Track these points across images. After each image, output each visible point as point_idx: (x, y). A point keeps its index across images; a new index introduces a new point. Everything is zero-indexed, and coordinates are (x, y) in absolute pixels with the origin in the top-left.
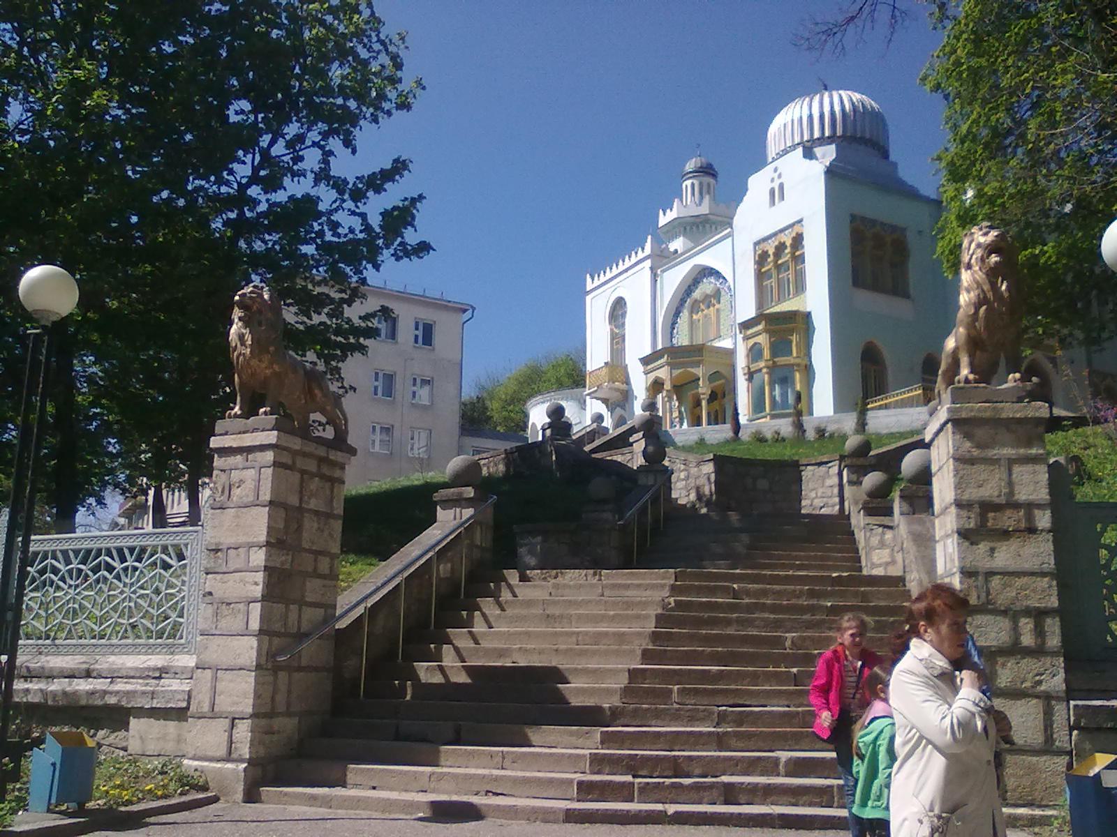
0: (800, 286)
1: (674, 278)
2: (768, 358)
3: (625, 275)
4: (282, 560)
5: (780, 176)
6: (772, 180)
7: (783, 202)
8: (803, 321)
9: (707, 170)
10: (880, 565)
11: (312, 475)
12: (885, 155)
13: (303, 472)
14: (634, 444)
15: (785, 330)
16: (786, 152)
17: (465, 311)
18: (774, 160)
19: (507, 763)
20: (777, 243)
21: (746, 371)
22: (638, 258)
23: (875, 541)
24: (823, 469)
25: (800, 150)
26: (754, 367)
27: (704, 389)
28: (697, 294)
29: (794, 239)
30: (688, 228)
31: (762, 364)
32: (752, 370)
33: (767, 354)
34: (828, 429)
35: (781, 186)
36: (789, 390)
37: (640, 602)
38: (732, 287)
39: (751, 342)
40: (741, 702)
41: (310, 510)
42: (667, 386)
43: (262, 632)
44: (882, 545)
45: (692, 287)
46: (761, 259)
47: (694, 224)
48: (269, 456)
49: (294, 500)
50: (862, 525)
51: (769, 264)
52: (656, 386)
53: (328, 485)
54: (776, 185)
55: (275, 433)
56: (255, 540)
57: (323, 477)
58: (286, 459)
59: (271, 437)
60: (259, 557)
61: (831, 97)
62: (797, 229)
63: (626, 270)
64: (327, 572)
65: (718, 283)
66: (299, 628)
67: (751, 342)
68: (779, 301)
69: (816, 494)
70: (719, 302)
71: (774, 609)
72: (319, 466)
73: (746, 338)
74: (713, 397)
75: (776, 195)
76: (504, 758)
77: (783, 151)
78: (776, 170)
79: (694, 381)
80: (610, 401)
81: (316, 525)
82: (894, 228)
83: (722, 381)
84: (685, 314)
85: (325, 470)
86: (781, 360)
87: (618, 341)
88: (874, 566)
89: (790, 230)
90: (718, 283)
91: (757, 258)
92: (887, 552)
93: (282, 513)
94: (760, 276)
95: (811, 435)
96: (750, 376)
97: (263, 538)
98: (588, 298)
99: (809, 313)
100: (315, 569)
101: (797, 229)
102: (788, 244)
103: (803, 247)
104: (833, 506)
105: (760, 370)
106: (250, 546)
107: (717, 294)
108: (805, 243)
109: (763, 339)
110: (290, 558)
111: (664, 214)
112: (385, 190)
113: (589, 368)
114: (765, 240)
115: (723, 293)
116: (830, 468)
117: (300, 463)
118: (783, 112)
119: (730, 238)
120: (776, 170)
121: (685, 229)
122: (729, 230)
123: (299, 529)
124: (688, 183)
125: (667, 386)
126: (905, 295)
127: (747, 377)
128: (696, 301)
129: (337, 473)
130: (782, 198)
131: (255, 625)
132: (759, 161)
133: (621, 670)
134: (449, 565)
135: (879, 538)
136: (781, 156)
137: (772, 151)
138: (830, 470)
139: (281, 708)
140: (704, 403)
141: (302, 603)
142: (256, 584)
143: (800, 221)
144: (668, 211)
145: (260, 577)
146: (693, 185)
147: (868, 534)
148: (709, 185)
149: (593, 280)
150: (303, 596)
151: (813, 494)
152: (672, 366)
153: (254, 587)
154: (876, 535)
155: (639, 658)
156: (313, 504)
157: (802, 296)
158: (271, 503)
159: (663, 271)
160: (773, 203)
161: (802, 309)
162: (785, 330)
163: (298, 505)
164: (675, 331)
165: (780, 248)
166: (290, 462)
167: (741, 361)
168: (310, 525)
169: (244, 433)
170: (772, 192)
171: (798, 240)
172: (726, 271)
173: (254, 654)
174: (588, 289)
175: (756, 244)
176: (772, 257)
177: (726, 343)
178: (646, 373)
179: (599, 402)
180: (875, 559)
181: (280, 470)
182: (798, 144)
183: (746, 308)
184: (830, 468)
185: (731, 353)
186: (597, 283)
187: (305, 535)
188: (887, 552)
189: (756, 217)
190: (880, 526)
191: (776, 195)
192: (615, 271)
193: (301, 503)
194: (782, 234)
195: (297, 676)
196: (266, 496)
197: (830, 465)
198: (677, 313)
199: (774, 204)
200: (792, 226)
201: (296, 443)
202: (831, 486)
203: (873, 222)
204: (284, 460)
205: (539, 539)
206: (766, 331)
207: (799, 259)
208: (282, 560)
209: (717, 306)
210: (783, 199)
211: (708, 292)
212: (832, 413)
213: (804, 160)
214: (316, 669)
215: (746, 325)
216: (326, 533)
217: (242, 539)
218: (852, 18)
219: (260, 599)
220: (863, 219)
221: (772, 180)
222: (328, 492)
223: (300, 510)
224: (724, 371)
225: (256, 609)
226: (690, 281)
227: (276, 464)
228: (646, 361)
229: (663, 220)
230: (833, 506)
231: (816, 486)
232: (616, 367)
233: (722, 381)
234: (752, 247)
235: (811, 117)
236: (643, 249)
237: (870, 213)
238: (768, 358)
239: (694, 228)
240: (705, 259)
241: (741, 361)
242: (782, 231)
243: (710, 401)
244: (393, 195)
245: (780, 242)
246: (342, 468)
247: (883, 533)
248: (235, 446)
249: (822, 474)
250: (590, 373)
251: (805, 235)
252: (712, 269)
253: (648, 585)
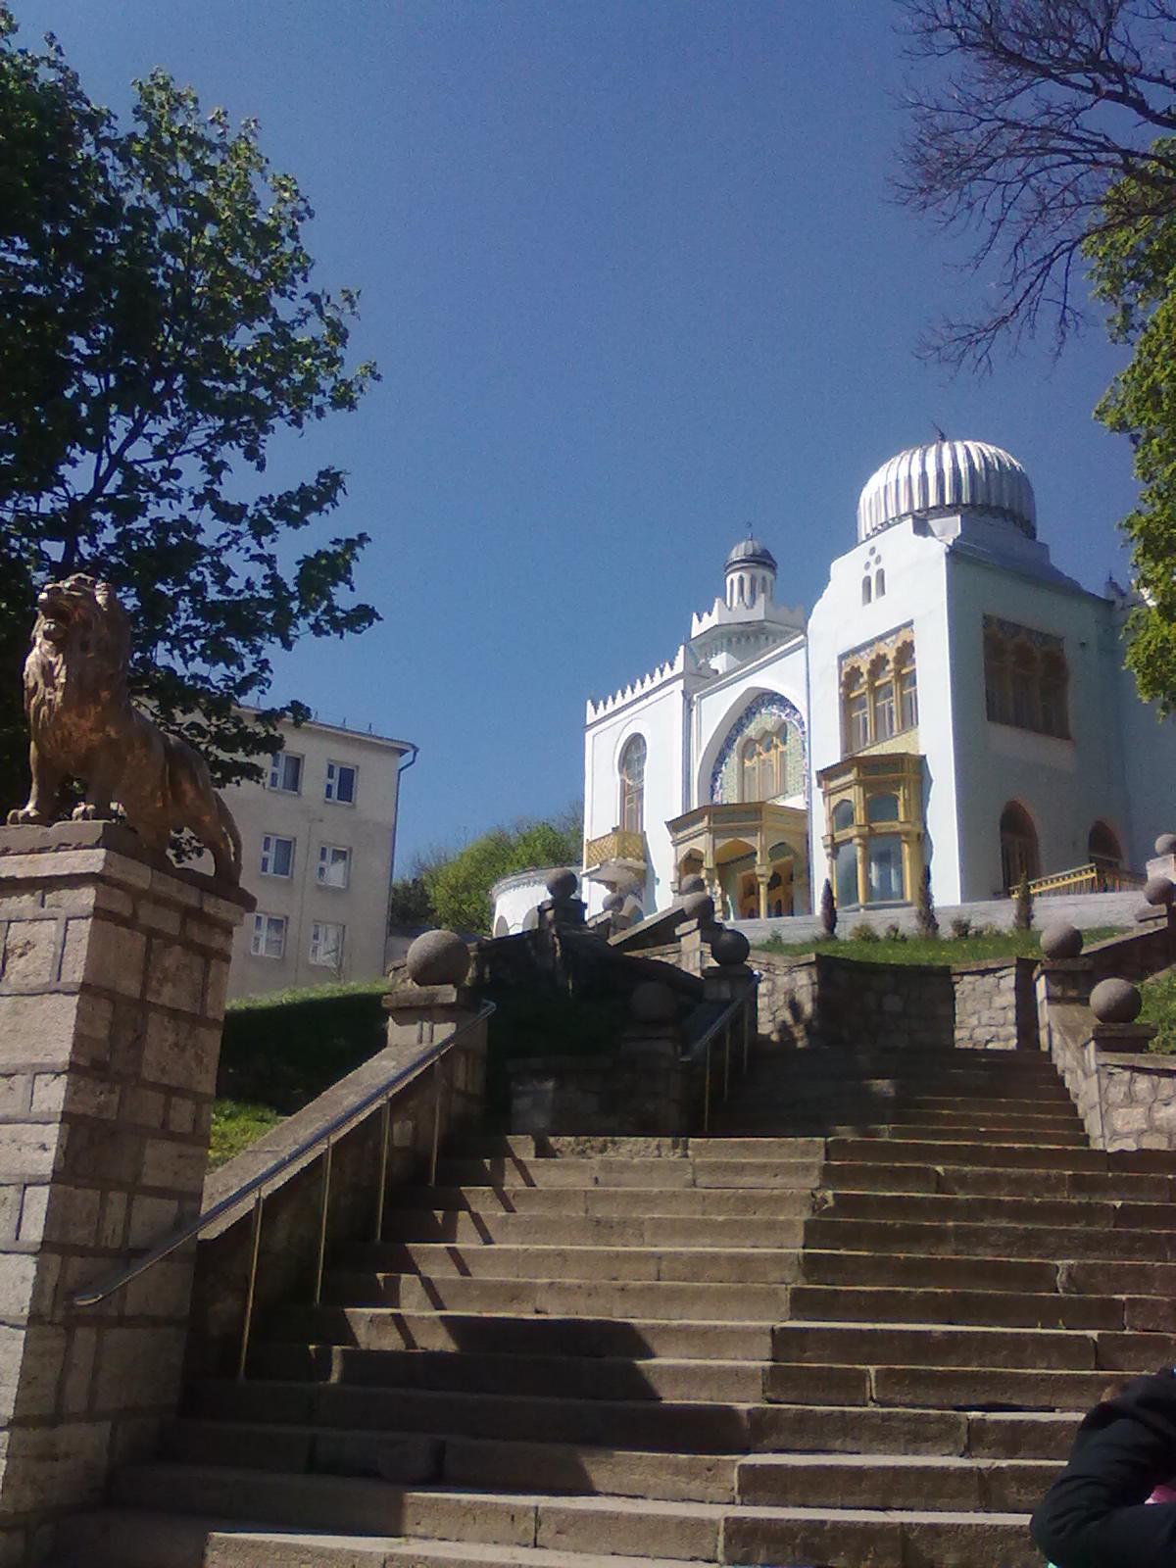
0: (909, 717)
1: (716, 708)
2: (863, 823)
3: (645, 702)
4: (100, 1100)
5: (878, 560)
6: (867, 566)
7: (883, 598)
8: (913, 771)
9: (761, 560)
10: (1127, 1135)
11: (170, 941)
12: (1031, 533)
13: (151, 933)
14: (683, 939)
15: (885, 782)
16: (887, 525)
17: (402, 752)
18: (869, 537)
19: (545, 1535)
20: (873, 657)
21: (829, 842)
22: (665, 678)
23: (1117, 1093)
24: (990, 980)
25: (909, 522)
26: (840, 836)
27: (762, 869)
28: (752, 730)
29: (900, 651)
30: (734, 640)
31: (852, 831)
32: (837, 840)
33: (859, 816)
34: (973, 924)
35: (881, 575)
36: (893, 871)
37: (770, 1198)
38: (805, 719)
39: (836, 799)
40: (1003, 1400)
41: (162, 1006)
42: (709, 863)
43: (46, 1246)
44: (1131, 1099)
45: (744, 721)
46: (850, 679)
47: (742, 633)
48: (87, 897)
49: (131, 986)
50: (1093, 1066)
51: (861, 688)
52: (690, 863)
53: (199, 961)
54: (872, 573)
55: (101, 852)
56: (48, 1060)
57: (189, 945)
58: (121, 905)
59: (93, 860)
60: (53, 1094)
61: (953, 449)
62: (904, 635)
63: (646, 695)
64: (187, 1127)
65: (784, 717)
66: (126, 1239)
67: (836, 799)
68: (877, 740)
69: (979, 1020)
70: (784, 742)
71: (1017, 1212)
72: (183, 923)
73: (828, 793)
74: (775, 882)
75: (873, 587)
76: (538, 1522)
77: (882, 525)
78: (872, 551)
79: (747, 856)
80: (619, 886)
81: (171, 1038)
82: (1046, 638)
83: (789, 858)
84: (733, 759)
85: (196, 933)
86: (882, 826)
87: (632, 797)
88: (1116, 1135)
89: (894, 637)
90: (784, 717)
91: (843, 679)
92: (1139, 1112)
93: (104, 1009)
94: (848, 704)
95: (946, 931)
96: (835, 848)
97: (63, 1055)
98: (589, 735)
99: (924, 757)
100: (164, 1124)
101: (904, 635)
102: (890, 657)
103: (914, 662)
104: (1007, 1039)
105: (850, 840)
106: (38, 1071)
107: (782, 731)
108: (916, 655)
109: (854, 795)
110: (115, 1098)
111: (700, 620)
112: (306, 523)
113: (587, 836)
114: (856, 651)
115: (789, 727)
116: (1001, 978)
117: (147, 915)
118: (882, 470)
119: (803, 650)
120: (872, 551)
121: (730, 640)
122: (802, 637)
123: (139, 1041)
124: (735, 576)
125: (709, 863)
126: (1064, 735)
127: (829, 850)
128: (751, 740)
129: (217, 941)
130: (882, 590)
131: (34, 1231)
132: (847, 540)
133: (760, 1331)
134: (410, 1124)
135: (1124, 1089)
136: (880, 532)
137: (865, 525)
138: (1002, 981)
139: (76, 1402)
140: (763, 889)
141: (135, 1189)
142: (44, 1147)
143: (910, 624)
144: (706, 615)
145: (52, 1134)
146: (741, 579)
147: (1105, 1082)
148: (764, 579)
149: (596, 708)
150: (138, 1176)
151: (974, 1021)
152: (716, 833)
153: (38, 1155)
154: (1121, 1082)
155: (785, 1307)
156: (167, 995)
157: (912, 733)
158: (85, 988)
159: (701, 697)
160: (867, 598)
161: (912, 752)
162: (885, 782)
163: (138, 996)
164: (718, 784)
165: (879, 663)
166: (127, 912)
167: (820, 827)
168: (160, 1037)
169: (41, 851)
170: (867, 583)
171: (906, 652)
172: (794, 694)
173: (27, 1292)
174: (589, 722)
175: (842, 657)
176: (866, 676)
177: (796, 802)
178: (676, 844)
179: (603, 887)
180: (1119, 1124)
181: (110, 926)
182: (905, 515)
183: (827, 749)
184: (1001, 978)
185: (802, 816)
186: (602, 712)
187: (149, 1054)
188: (1139, 1112)
189: (842, 619)
190: (1124, 1067)
191: (873, 587)
192: (629, 696)
193: (143, 992)
194: (882, 644)
195: (116, 1336)
196: (75, 973)
197: (1002, 973)
198: (721, 759)
199: (869, 600)
200: (896, 631)
201: (141, 876)
202: (1004, 1008)
203: (1017, 628)
204: (115, 907)
205: (550, 1085)
206: (858, 782)
207: (907, 679)
208: (100, 1100)
209: (782, 748)
210: (883, 592)
211: (769, 727)
212: (958, 901)
213: (915, 536)
214: (154, 1322)
215: (826, 775)
216: (190, 1053)
217: (21, 1058)
218: (1005, 320)
219: (49, 1179)
220: (1002, 623)
221: (867, 566)
222: (197, 975)
223: (142, 1005)
224: (791, 842)
225: (39, 1200)
226: (741, 712)
227: (99, 913)
228: (675, 826)
229: (698, 628)
230: (1007, 1039)
231: (978, 1007)
232: (629, 835)
233: (789, 858)
234: (835, 662)
235: (924, 475)
236: (672, 666)
237: (1012, 615)
238: (863, 823)
239: (743, 640)
240: (764, 680)
241: (820, 827)
242: (881, 638)
243: (771, 887)
244: (317, 535)
245: (878, 656)
246: (228, 932)
247: (1132, 1081)
248: (19, 876)
249: (987, 988)
250: (590, 843)
251: (915, 644)
252: (777, 694)
253: (779, 1166)
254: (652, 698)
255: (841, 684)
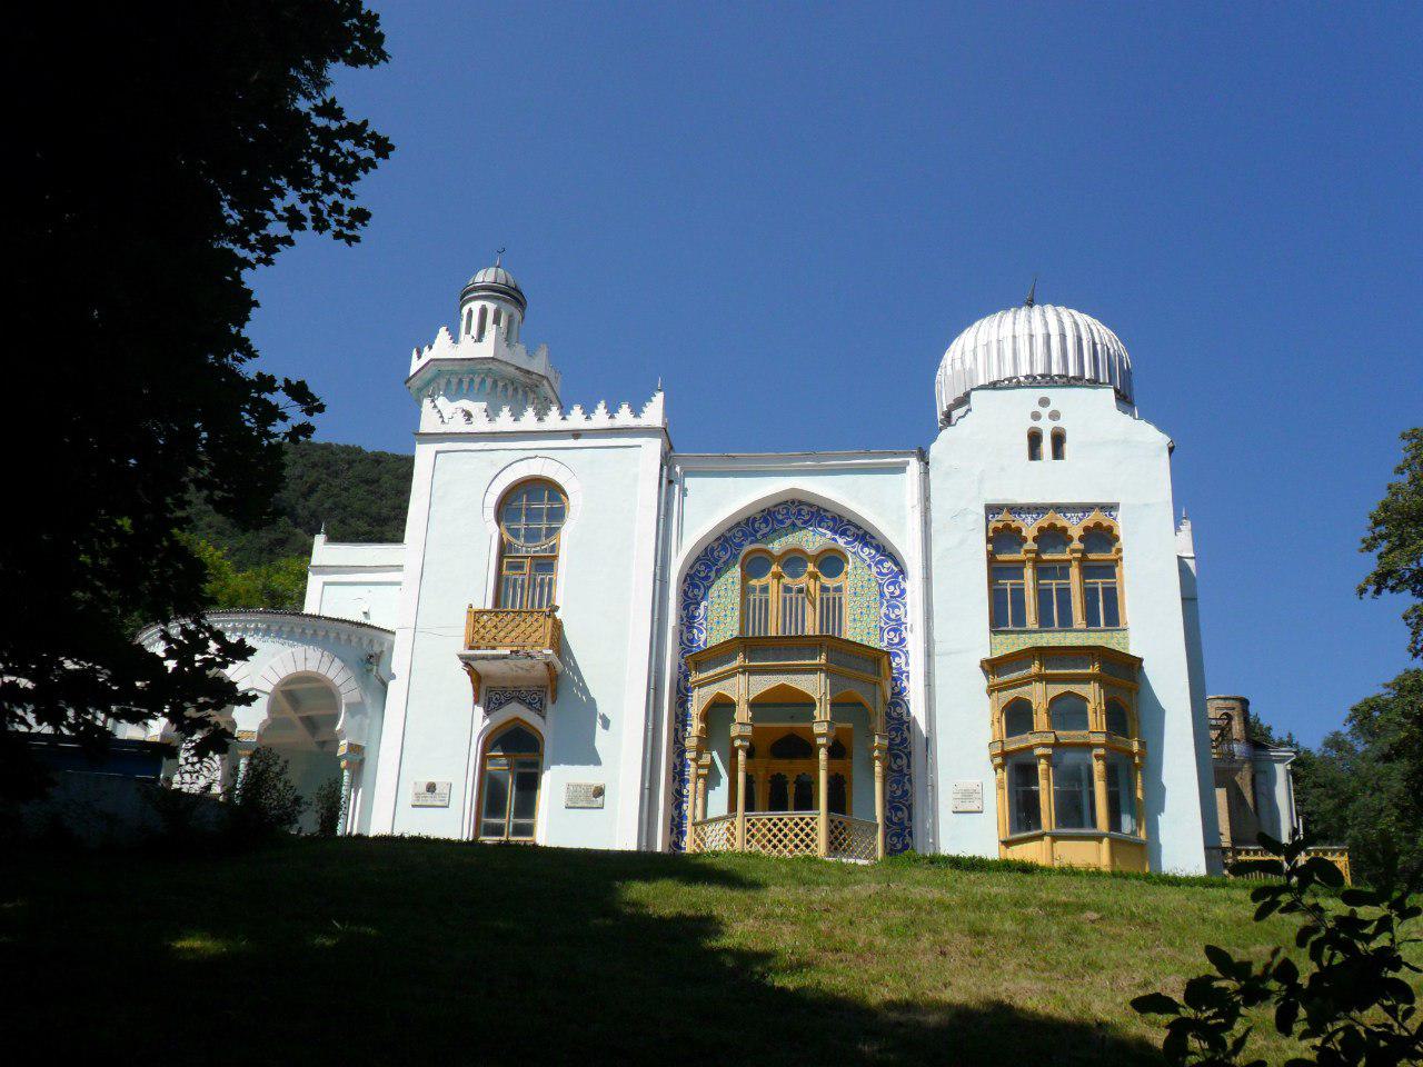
5: (1055, 415)
9: (510, 295)
30: (500, 384)
54: (1046, 427)
63: (576, 434)
91: (991, 534)
120: (1044, 402)
124: (476, 306)
130: (1058, 453)
171: (1101, 537)
179: (468, 678)
221: (1036, 416)
235: (1048, 337)
236: (636, 412)
251: (1121, 529)
254: (581, 442)
255: (989, 540)
